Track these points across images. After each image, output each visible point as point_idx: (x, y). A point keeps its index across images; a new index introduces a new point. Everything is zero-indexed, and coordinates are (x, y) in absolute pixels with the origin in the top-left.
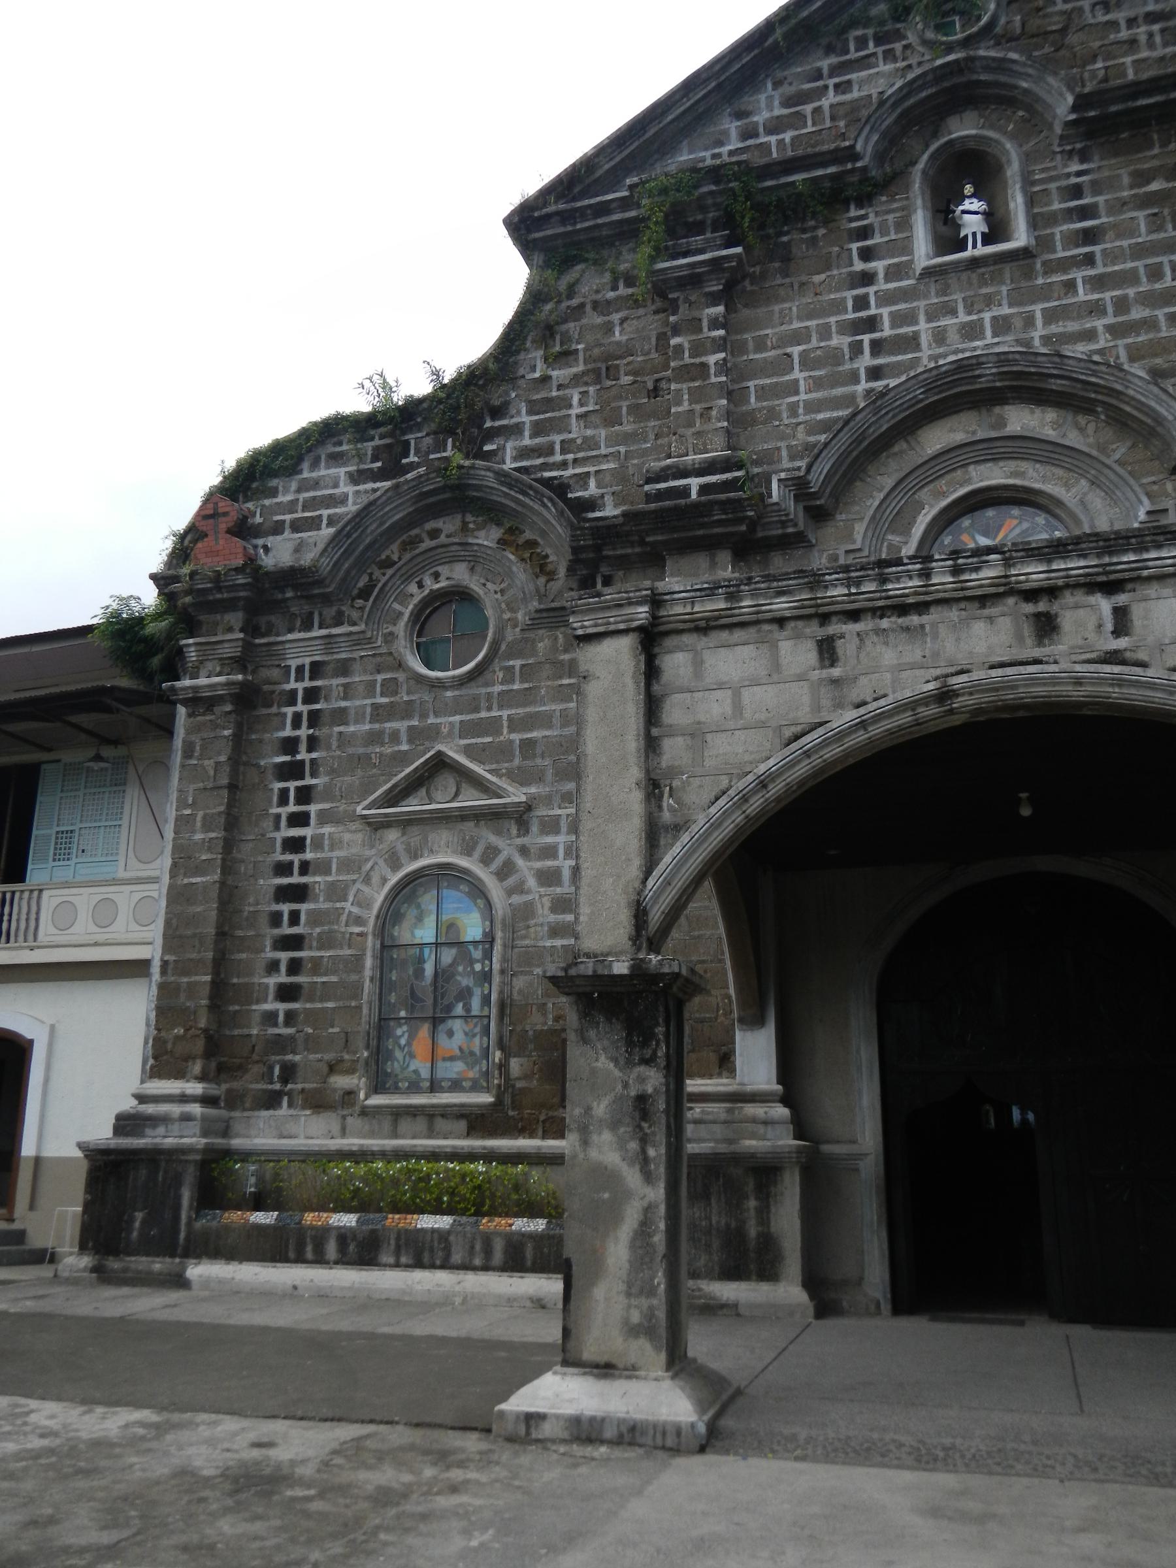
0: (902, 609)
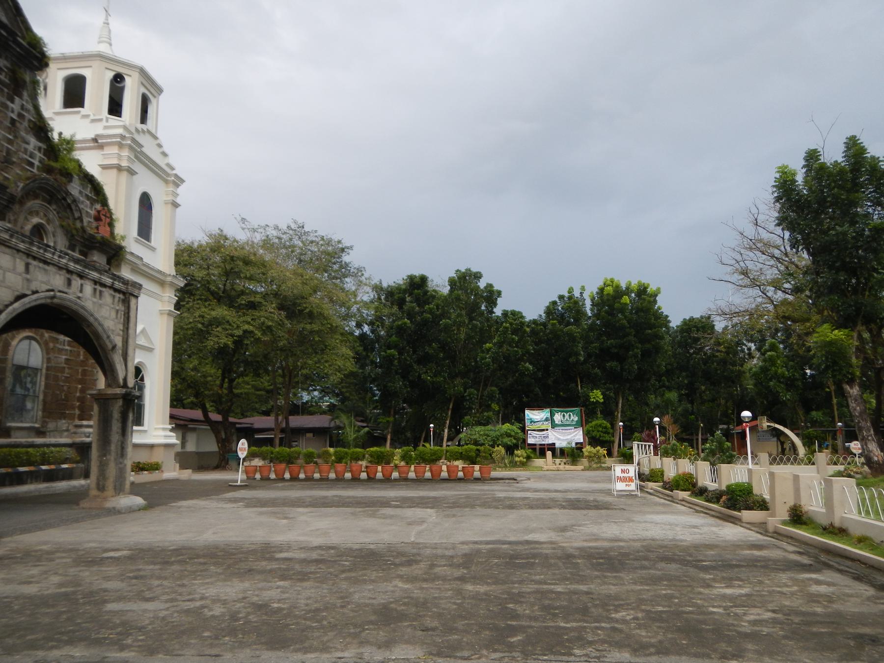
0: (46, 262)
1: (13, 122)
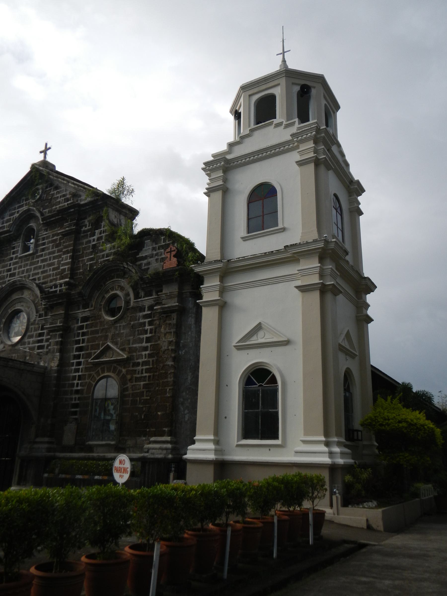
1: (94, 246)
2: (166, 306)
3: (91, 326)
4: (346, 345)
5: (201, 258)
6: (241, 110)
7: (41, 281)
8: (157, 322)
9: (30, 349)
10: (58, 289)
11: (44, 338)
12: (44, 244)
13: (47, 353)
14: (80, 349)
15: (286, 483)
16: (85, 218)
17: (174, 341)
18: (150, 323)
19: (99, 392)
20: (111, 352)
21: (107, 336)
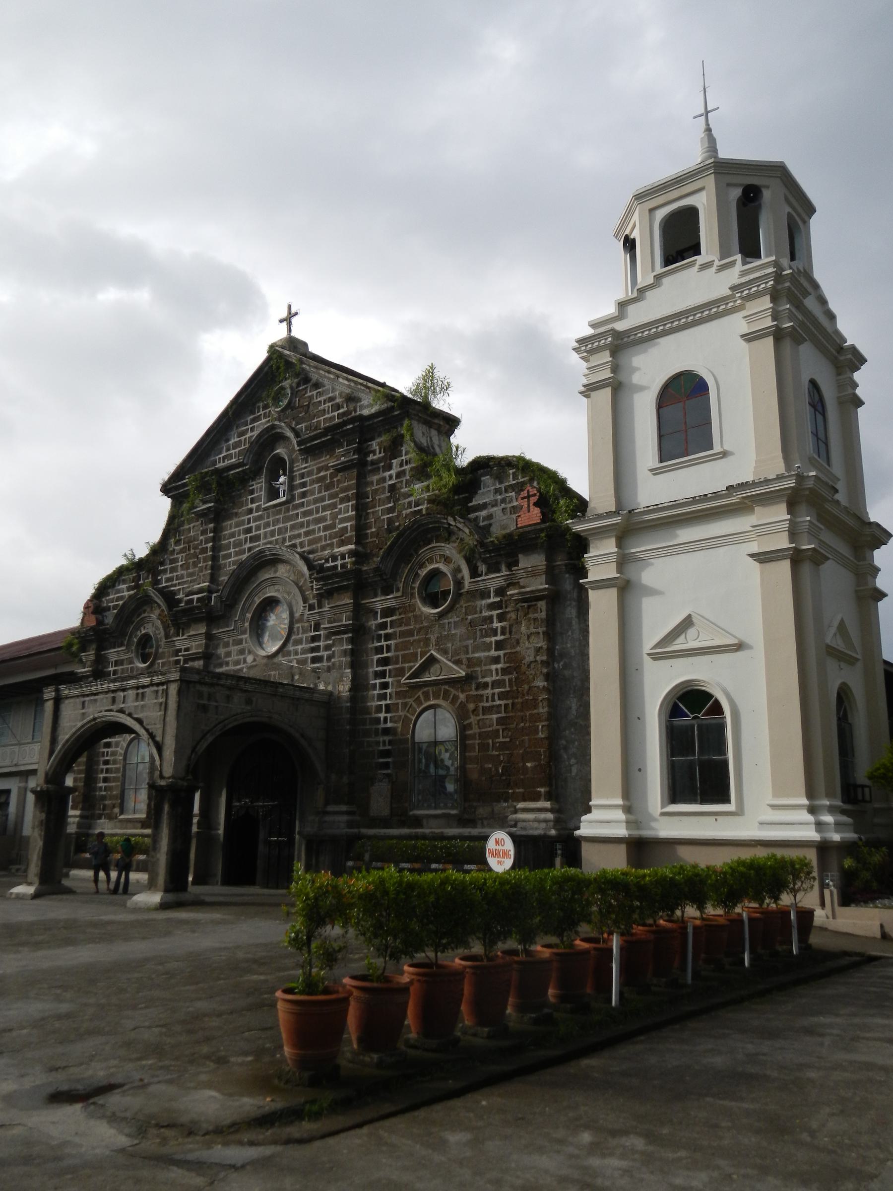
0: (95, 694)
1: (392, 488)
2: (528, 589)
3: (400, 623)
4: (839, 644)
5: (580, 506)
6: (636, 234)
7: (306, 549)
8: (513, 616)
9: (298, 662)
10: (339, 562)
11: (321, 644)
12: (304, 485)
13: (329, 669)
14: (385, 662)
15: (753, 866)
16: (373, 439)
17: (545, 647)
18: (501, 618)
19: (423, 733)
20: (437, 666)
21: (429, 639)
